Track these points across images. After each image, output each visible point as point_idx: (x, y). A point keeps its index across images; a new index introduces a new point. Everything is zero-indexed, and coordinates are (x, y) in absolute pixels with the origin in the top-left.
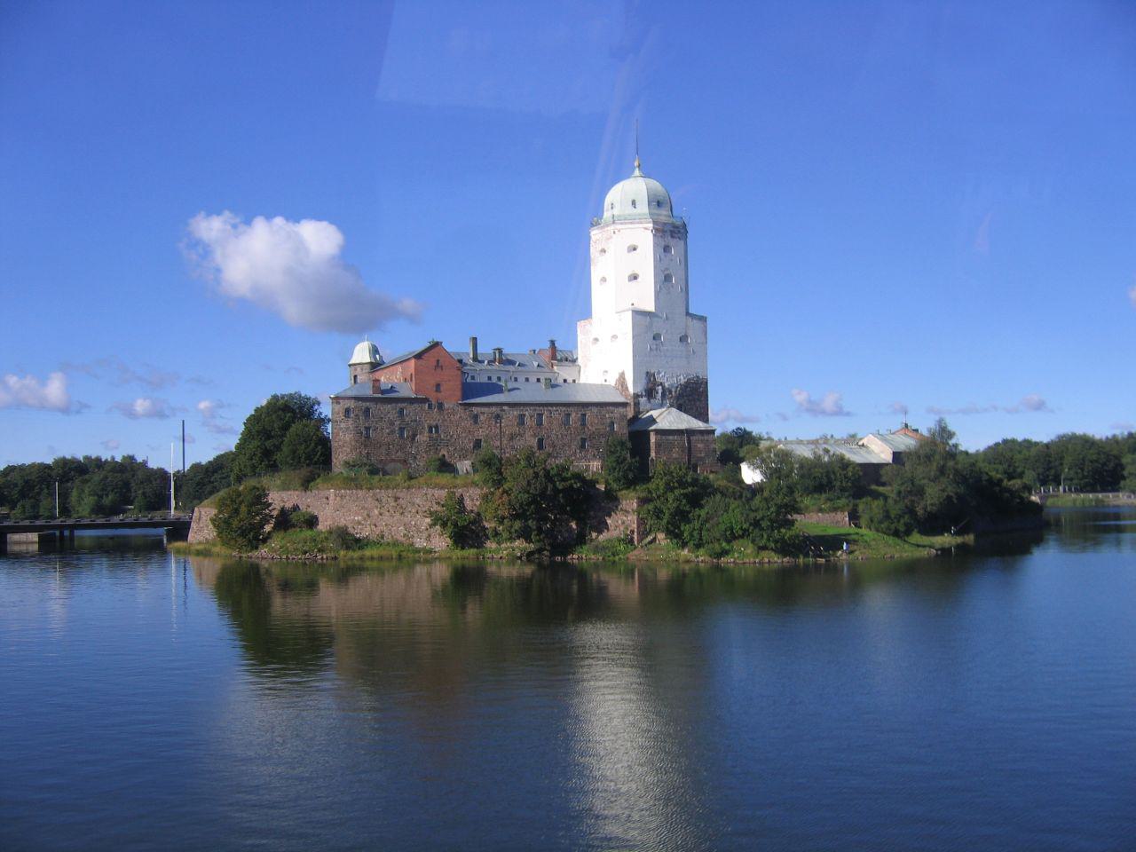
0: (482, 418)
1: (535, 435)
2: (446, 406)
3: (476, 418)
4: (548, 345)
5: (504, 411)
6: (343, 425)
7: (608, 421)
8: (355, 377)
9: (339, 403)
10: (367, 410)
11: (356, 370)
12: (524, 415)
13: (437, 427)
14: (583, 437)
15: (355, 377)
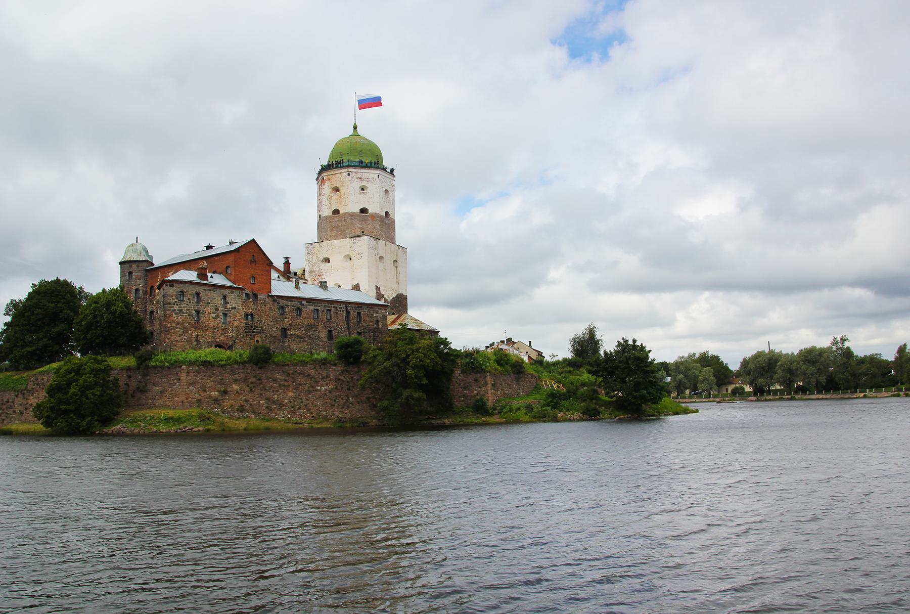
0: (287, 310)
1: (325, 327)
2: (260, 297)
3: (283, 308)
4: (284, 261)
5: (303, 305)
6: (176, 307)
7: (375, 319)
8: (130, 273)
9: (173, 286)
10: (198, 294)
11: (131, 266)
12: (318, 310)
13: (252, 315)
14: (359, 331)
15: (130, 273)
